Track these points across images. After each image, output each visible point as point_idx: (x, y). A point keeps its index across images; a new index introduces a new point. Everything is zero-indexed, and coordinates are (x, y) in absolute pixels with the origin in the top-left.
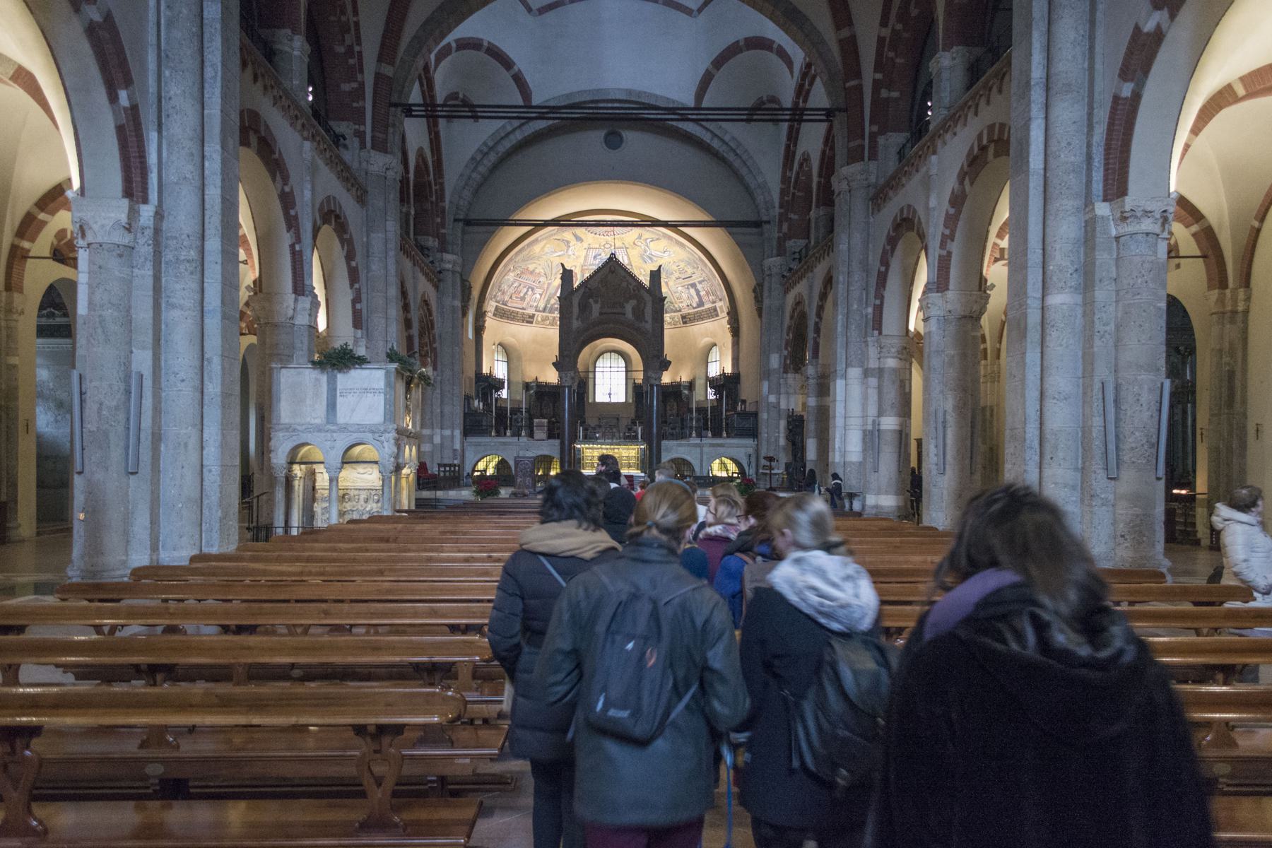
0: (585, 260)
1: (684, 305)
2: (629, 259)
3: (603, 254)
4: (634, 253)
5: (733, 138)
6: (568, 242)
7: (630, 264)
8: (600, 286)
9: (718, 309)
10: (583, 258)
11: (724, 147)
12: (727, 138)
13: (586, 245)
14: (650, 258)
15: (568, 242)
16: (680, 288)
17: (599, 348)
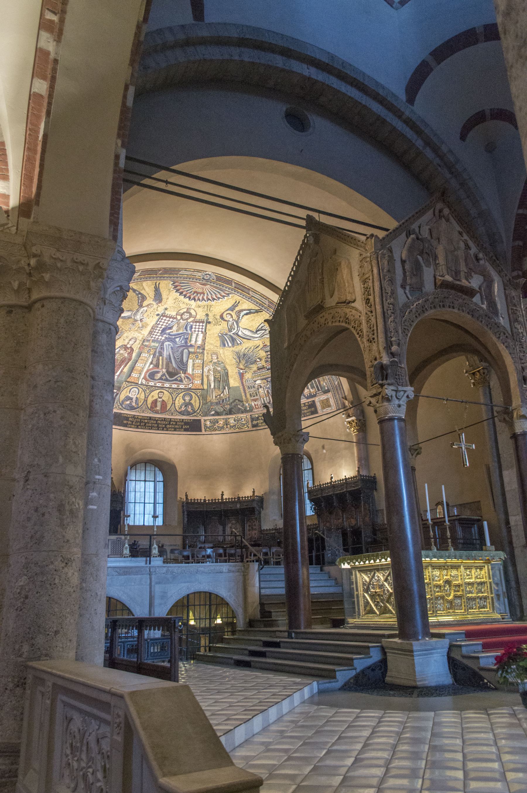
0: (151, 333)
1: (259, 403)
2: (204, 340)
3: (175, 328)
4: (214, 331)
5: (450, 151)
6: (144, 298)
7: (202, 347)
8: (429, 238)
9: (318, 405)
10: (149, 328)
11: (437, 161)
12: (444, 149)
13: (161, 310)
14: (233, 340)
15: (144, 298)
16: (258, 382)
17: (136, 454)
